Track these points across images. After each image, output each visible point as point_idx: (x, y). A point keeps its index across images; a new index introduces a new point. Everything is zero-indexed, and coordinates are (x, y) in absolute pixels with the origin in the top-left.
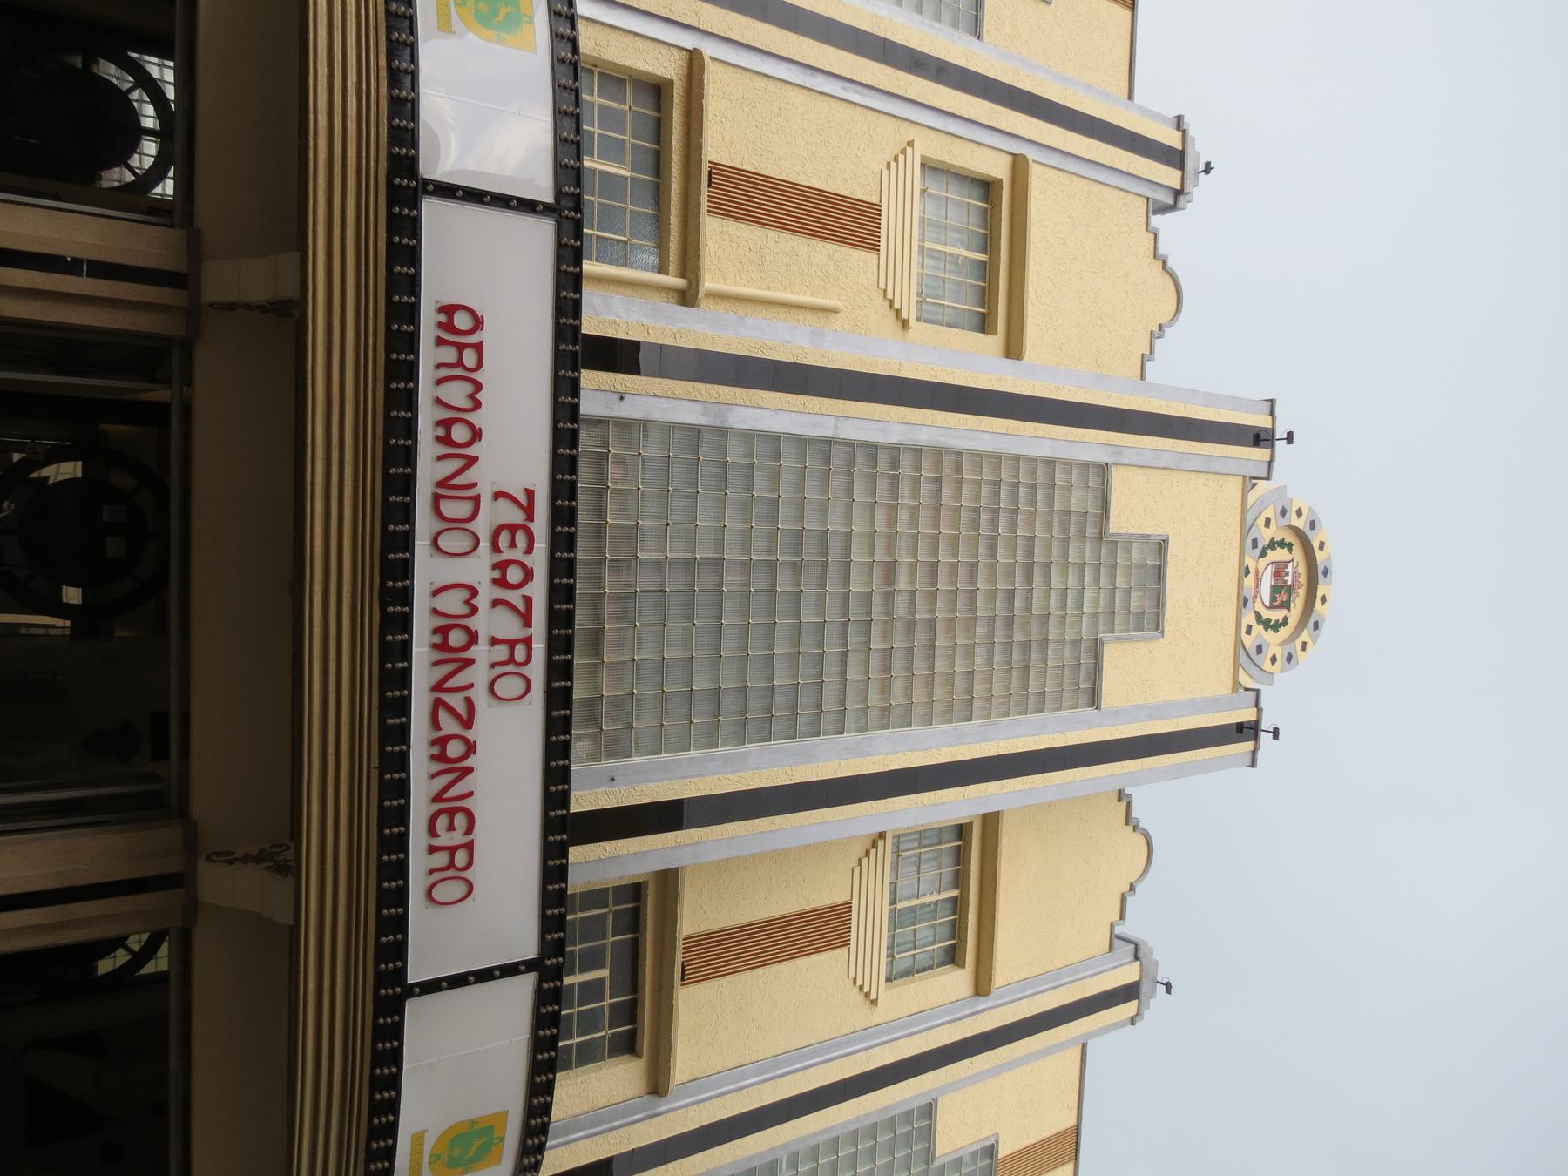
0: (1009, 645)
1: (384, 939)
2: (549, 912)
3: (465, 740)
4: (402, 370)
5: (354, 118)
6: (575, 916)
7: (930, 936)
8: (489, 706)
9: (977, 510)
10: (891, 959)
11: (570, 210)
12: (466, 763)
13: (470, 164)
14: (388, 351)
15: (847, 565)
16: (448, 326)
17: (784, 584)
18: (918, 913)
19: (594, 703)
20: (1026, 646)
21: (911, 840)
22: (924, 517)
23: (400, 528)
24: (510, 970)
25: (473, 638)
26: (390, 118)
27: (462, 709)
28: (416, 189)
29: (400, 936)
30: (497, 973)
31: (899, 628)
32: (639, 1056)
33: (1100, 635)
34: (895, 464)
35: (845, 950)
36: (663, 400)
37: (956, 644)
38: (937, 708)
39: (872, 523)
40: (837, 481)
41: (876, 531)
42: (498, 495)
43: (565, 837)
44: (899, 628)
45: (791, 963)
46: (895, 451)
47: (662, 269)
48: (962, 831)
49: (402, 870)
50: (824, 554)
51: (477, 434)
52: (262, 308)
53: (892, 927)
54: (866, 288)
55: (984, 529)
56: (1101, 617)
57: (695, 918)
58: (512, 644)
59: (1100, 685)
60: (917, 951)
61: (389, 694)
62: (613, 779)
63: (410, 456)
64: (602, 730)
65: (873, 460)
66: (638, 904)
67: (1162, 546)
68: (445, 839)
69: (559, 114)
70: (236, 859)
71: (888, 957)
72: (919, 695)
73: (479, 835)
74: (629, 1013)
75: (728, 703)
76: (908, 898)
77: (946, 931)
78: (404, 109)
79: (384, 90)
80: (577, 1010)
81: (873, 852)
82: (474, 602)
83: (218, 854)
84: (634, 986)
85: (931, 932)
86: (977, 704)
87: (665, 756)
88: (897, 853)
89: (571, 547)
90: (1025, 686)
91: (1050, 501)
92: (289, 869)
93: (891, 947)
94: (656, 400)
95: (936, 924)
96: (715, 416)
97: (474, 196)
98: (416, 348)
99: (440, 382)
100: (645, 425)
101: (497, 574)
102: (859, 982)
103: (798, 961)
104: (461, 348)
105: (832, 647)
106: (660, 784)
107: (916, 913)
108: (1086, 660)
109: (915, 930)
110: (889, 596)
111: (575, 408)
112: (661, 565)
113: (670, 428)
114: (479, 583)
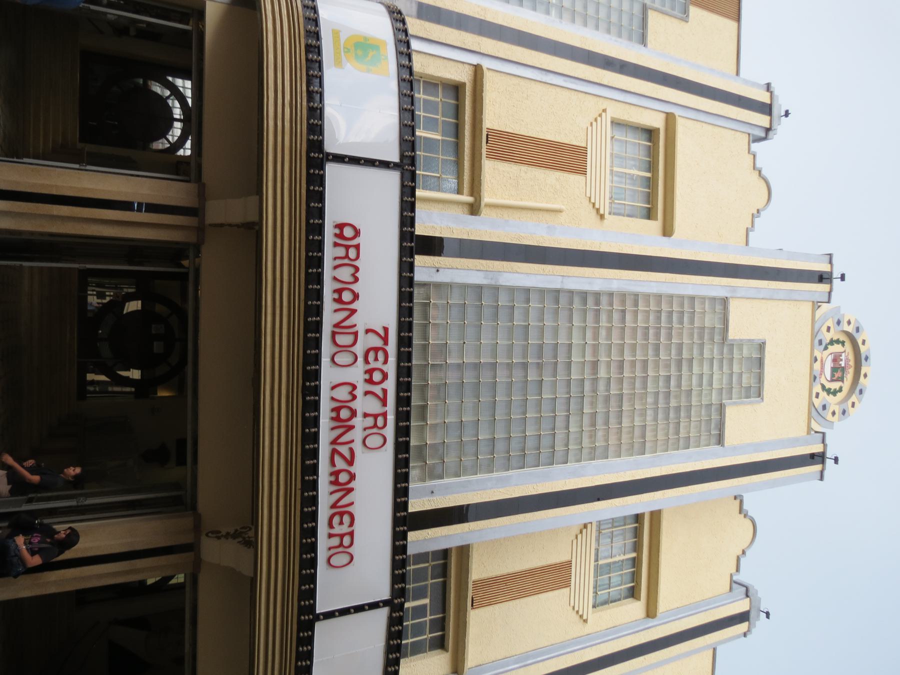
0: (667, 410)
1: (303, 588)
2: (397, 572)
3: (349, 472)
4: (315, 262)
5: (288, 120)
6: (410, 568)
7: (619, 582)
8: (363, 453)
9: (647, 328)
10: (595, 594)
11: (409, 165)
12: (350, 486)
13: (352, 139)
14: (307, 251)
15: (569, 364)
16: (341, 236)
17: (532, 376)
18: (612, 566)
19: (421, 449)
20: (678, 409)
21: (607, 524)
22: (615, 333)
23: (313, 352)
24: (374, 606)
25: (354, 413)
26: (308, 119)
27: (348, 455)
28: (322, 159)
29: (312, 586)
30: (367, 607)
31: (600, 401)
32: (447, 651)
33: (724, 401)
34: (597, 302)
35: (568, 589)
36: (462, 271)
37: (635, 409)
38: (624, 447)
39: (584, 339)
40: (563, 315)
41: (586, 343)
42: (368, 331)
43: (406, 528)
44: (600, 401)
45: (536, 597)
46: (597, 295)
47: (459, 191)
48: (638, 518)
49: (313, 548)
50: (555, 357)
51: (356, 296)
52: (238, 226)
53: (596, 575)
54: (578, 197)
55: (652, 340)
56: (724, 391)
57: (479, 570)
58: (376, 416)
59: (723, 432)
60: (611, 590)
61: (307, 447)
62: (432, 492)
63: (319, 311)
64: (426, 463)
65: (584, 301)
66: (446, 561)
67: (762, 346)
68: (338, 530)
69: (402, 110)
70: (222, 536)
71: (593, 593)
72: (613, 440)
73: (357, 527)
74: (441, 624)
75: (500, 446)
76: (605, 558)
77: (629, 577)
78: (316, 113)
79: (305, 103)
80: (411, 622)
81: (584, 531)
82: (355, 392)
83: (212, 532)
84: (444, 609)
85: (620, 579)
86: (648, 445)
87: (463, 478)
88: (599, 531)
89: (409, 360)
90: (677, 432)
91: (692, 321)
92: (251, 544)
93: (595, 587)
94: (457, 270)
95: (622, 574)
96: (492, 279)
97: (355, 161)
98: (322, 249)
99: (336, 267)
100: (450, 286)
101: (367, 377)
102: (576, 609)
103: (540, 596)
104: (347, 247)
105: (561, 413)
106: (460, 495)
107: (610, 567)
108: (715, 416)
109: (610, 577)
110: (595, 381)
111: (411, 279)
112: (460, 367)
113: (464, 287)
114: (358, 382)
